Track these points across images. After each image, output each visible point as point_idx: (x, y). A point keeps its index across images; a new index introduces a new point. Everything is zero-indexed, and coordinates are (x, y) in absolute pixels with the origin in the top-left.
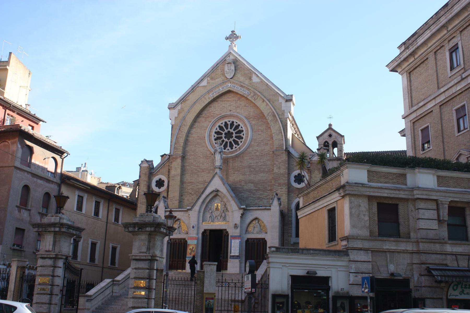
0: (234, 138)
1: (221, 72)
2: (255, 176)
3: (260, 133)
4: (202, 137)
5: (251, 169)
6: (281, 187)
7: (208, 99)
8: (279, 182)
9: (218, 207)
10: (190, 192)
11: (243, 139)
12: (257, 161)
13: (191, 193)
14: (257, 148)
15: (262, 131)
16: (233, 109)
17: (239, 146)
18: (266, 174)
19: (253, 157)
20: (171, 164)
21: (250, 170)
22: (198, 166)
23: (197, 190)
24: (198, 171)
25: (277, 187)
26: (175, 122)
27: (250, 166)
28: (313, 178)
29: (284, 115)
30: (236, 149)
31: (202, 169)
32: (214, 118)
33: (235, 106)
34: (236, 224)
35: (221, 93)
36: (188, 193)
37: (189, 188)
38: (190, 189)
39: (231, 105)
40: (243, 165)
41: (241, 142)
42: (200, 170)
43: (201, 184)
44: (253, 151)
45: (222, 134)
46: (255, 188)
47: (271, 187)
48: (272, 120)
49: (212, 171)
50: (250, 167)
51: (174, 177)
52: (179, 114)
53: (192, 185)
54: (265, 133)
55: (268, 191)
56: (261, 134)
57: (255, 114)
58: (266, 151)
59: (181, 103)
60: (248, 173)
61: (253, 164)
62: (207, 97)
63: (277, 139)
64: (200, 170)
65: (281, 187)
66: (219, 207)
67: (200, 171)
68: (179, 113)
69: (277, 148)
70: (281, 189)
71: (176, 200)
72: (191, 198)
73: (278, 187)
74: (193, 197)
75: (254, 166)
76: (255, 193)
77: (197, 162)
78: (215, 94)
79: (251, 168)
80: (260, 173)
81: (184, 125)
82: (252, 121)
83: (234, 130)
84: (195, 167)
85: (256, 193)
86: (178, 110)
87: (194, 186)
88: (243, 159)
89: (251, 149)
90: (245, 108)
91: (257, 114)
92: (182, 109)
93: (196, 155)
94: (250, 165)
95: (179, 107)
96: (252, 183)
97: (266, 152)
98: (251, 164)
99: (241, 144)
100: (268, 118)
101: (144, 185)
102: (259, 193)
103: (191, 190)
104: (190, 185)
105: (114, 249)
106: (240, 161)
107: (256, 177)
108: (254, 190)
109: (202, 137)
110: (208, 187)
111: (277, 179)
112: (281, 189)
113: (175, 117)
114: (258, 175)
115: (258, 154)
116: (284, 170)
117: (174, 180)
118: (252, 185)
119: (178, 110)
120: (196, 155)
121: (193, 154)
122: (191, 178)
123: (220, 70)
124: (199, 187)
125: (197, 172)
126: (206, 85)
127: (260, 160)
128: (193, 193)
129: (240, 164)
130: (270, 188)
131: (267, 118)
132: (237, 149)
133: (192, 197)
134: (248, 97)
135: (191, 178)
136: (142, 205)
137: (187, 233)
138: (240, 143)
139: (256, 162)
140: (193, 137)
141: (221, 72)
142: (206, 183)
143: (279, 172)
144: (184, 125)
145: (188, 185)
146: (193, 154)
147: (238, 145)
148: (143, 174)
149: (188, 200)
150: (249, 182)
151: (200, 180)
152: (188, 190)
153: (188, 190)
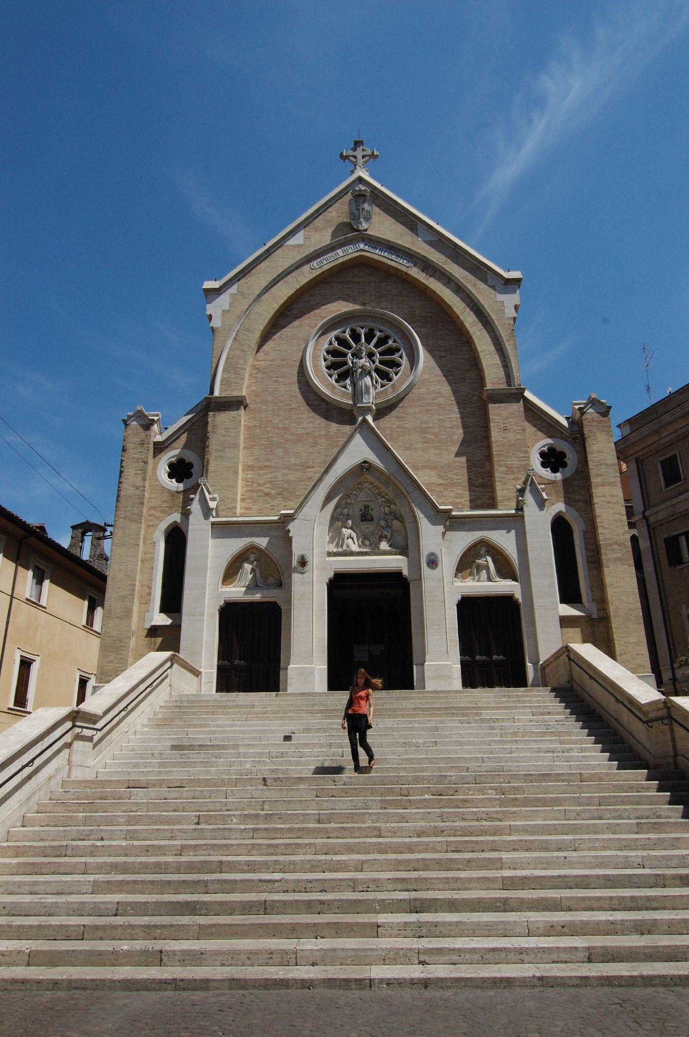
0: (377, 363)
1: (339, 217)
2: (438, 452)
3: (443, 354)
4: (293, 361)
5: (428, 436)
6: (513, 477)
7: (307, 275)
8: (509, 463)
9: (368, 511)
10: (267, 490)
11: (402, 367)
12: (442, 417)
13: (267, 494)
14: (439, 387)
15: (446, 350)
16: (372, 301)
17: (391, 383)
18: (467, 447)
19: (429, 408)
20: (214, 420)
21: (425, 437)
22: (284, 429)
23: (285, 486)
24: (287, 440)
25: (504, 476)
26: (223, 321)
27: (425, 428)
28: (595, 455)
29: (504, 313)
30: (384, 388)
31: (297, 435)
32: (323, 318)
33: (375, 296)
34: (432, 554)
35: (340, 261)
36: (261, 494)
37: (262, 481)
38: (265, 484)
39: (364, 292)
40: (406, 426)
41: (396, 374)
42: (290, 437)
43: (295, 470)
44: (427, 394)
45: (345, 355)
46: (440, 481)
47: (482, 479)
48: (474, 322)
49: (323, 440)
50: (423, 430)
51: (221, 451)
52: (231, 304)
53: (271, 473)
54: (457, 354)
55: (477, 487)
56: (445, 357)
57: (427, 313)
58: (461, 394)
59: (239, 280)
60: (419, 446)
61: (430, 425)
62: (306, 268)
63: (492, 365)
64: (290, 437)
65: (513, 477)
66: (373, 513)
67: (292, 440)
68: (234, 300)
69: (493, 384)
70: (513, 479)
71: (228, 508)
72: (269, 506)
73: (506, 474)
74: (273, 503)
75: (433, 427)
76: (441, 492)
77: (282, 418)
78: (325, 262)
79: (427, 434)
80: (452, 446)
81: (249, 330)
82: (421, 327)
83: (376, 346)
84: (276, 431)
85: (446, 492)
86: (230, 294)
87: (276, 477)
88: (404, 413)
89: (423, 390)
90: (401, 298)
91: (431, 312)
92: (240, 293)
93: (281, 402)
94: (424, 426)
95: (234, 289)
96: (433, 467)
97: (462, 396)
98: (426, 423)
99: (395, 378)
100: (465, 317)
101: (137, 470)
102: (453, 494)
103: (268, 485)
104: (265, 474)
105: (26, 665)
106: (397, 417)
107: (440, 454)
108: (438, 485)
109: (293, 361)
110: (343, 456)
111: (501, 458)
112: (513, 479)
113: (223, 311)
114: (447, 450)
115: (441, 400)
116: (519, 437)
117: (221, 457)
118: (434, 473)
119: (230, 294)
120: (281, 402)
121: (270, 399)
122: (268, 457)
123: (334, 214)
124: (292, 477)
125: (283, 441)
126: (302, 243)
127: (449, 414)
128: (273, 492)
129: (398, 423)
130: (480, 481)
131: (462, 318)
132: (387, 389)
133: (273, 503)
134: (410, 272)
135: (268, 457)
136: (130, 521)
137: (281, 585)
138: (392, 375)
139: (439, 419)
140: (271, 361)
141: (339, 217)
142: (308, 467)
143: (505, 441)
144: (249, 330)
145: (259, 474)
146: (270, 399)
147: (390, 380)
148: (134, 444)
149: (261, 510)
150: (424, 467)
151: (292, 460)
152: (259, 485)
153: (259, 485)
